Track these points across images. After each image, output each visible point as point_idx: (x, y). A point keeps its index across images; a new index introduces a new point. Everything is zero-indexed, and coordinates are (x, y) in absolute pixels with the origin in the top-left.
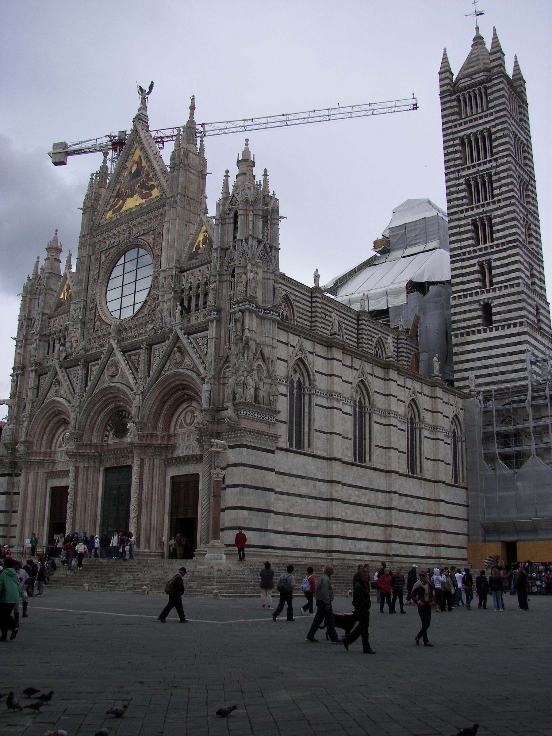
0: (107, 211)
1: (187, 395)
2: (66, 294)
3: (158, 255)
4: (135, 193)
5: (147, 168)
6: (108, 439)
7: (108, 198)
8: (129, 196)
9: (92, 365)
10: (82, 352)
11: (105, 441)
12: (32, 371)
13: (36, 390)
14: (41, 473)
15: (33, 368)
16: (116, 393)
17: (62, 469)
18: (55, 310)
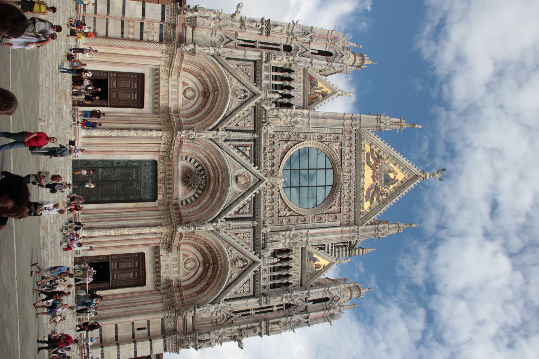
0: (371, 145)
1: (209, 267)
2: (320, 91)
3: (320, 219)
4: (374, 181)
5: (387, 191)
6: (183, 160)
7: (380, 147)
8: (374, 172)
9: (251, 146)
10: (265, 131)
11: (182, 157)
12: (261, 56)
13: (242, 58)
14: (161, 64)
15: (264, 60)
16: (222, 186)
17: (161, 88)
18: (309, 75)
